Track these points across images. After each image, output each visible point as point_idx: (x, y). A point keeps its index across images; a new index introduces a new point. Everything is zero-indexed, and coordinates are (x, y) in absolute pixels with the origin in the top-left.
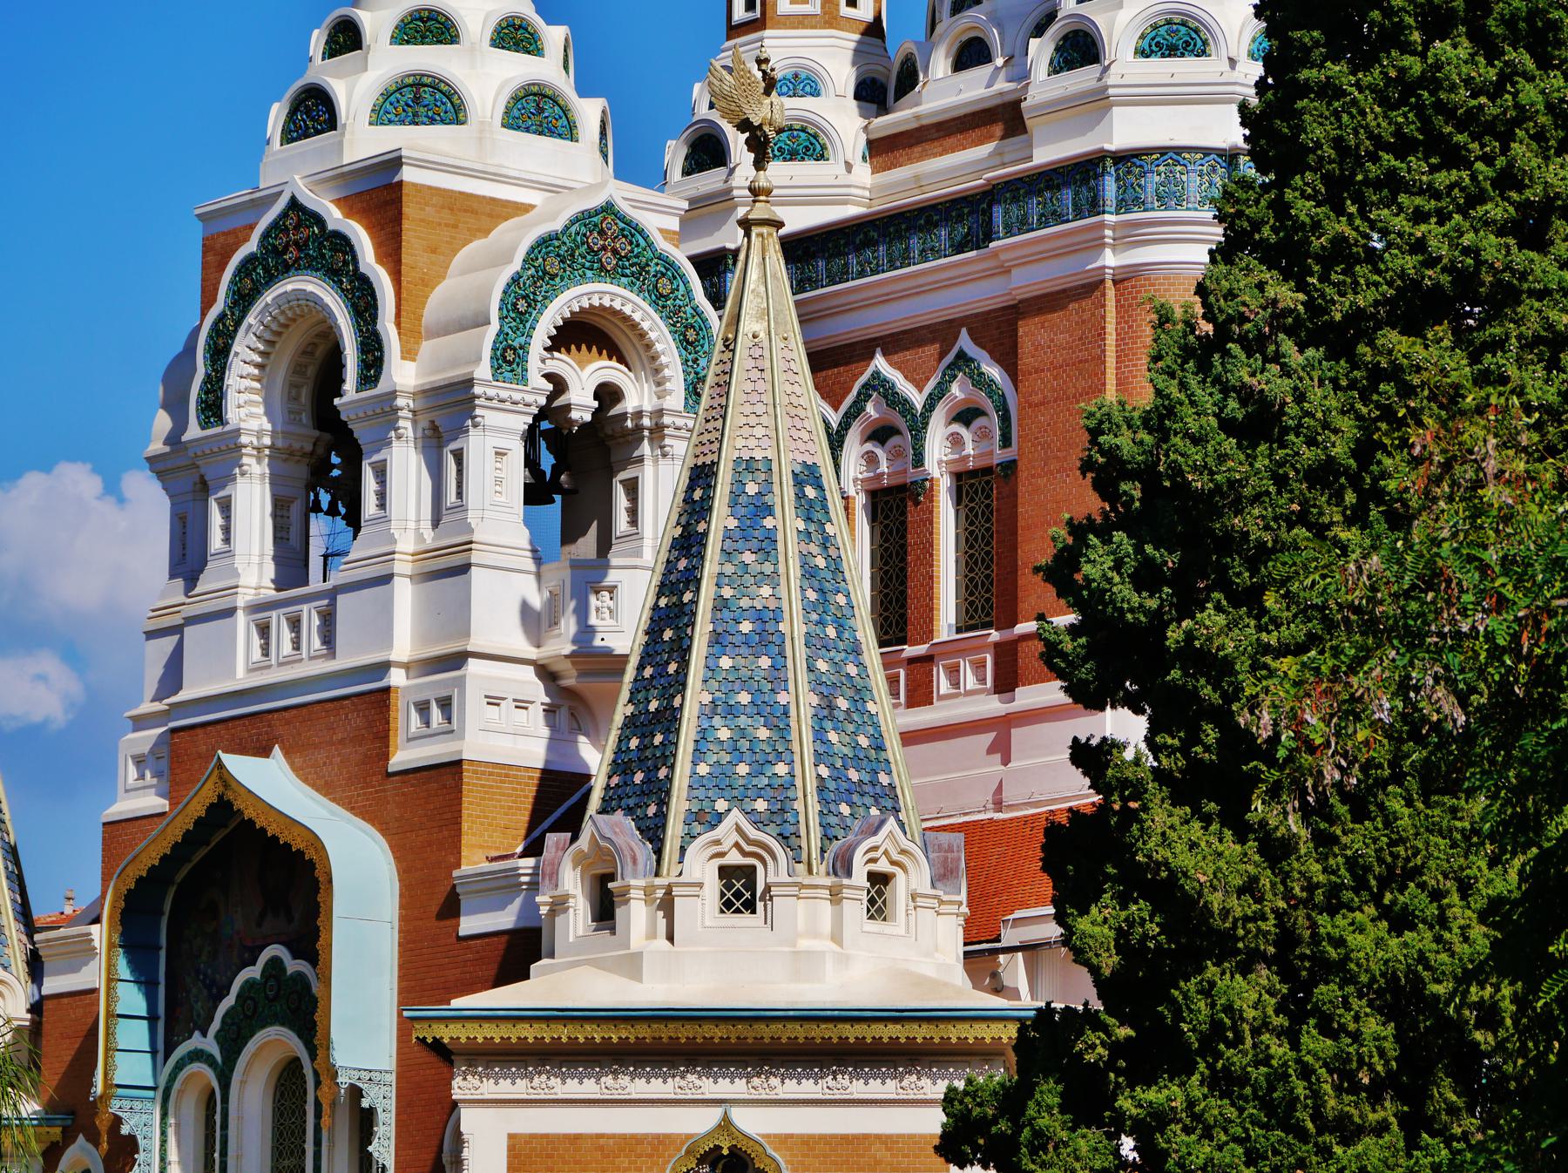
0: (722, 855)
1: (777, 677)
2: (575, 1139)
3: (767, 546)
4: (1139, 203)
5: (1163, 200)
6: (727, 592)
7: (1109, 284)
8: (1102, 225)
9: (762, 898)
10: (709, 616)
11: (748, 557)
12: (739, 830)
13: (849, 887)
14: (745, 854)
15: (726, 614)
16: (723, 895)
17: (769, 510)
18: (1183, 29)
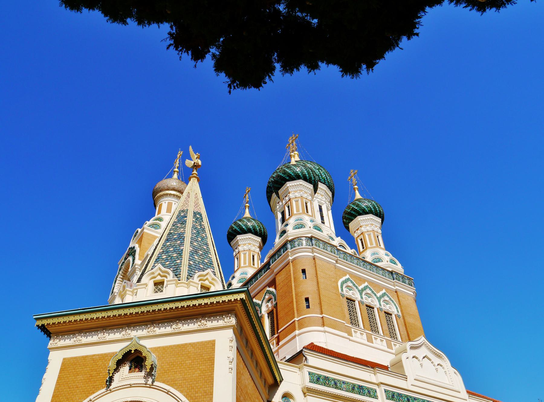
0: (155, 277)
1: (182, 244)
2: (84, 358)
3: (184, 223)
4: (294, 247)
5: (299, 245)
6: (172, 232)
7: (291, 263)
8: (288, 252)
9: (165, 288)
10: (166, 236)
11: (179, 225)
12: (160, 269)
13: (192, 282)
14: (162, 276)
15: (171, 235)
16: (155, 290)
17: (186, 217)
18: (301, 225)
